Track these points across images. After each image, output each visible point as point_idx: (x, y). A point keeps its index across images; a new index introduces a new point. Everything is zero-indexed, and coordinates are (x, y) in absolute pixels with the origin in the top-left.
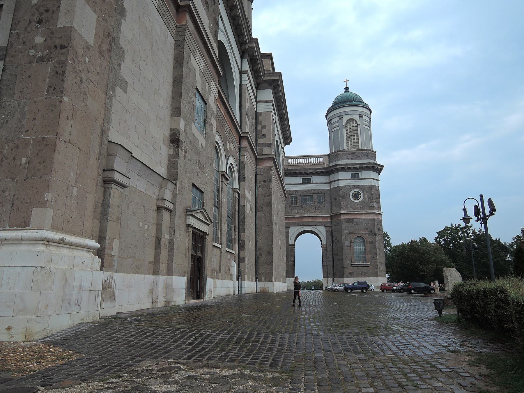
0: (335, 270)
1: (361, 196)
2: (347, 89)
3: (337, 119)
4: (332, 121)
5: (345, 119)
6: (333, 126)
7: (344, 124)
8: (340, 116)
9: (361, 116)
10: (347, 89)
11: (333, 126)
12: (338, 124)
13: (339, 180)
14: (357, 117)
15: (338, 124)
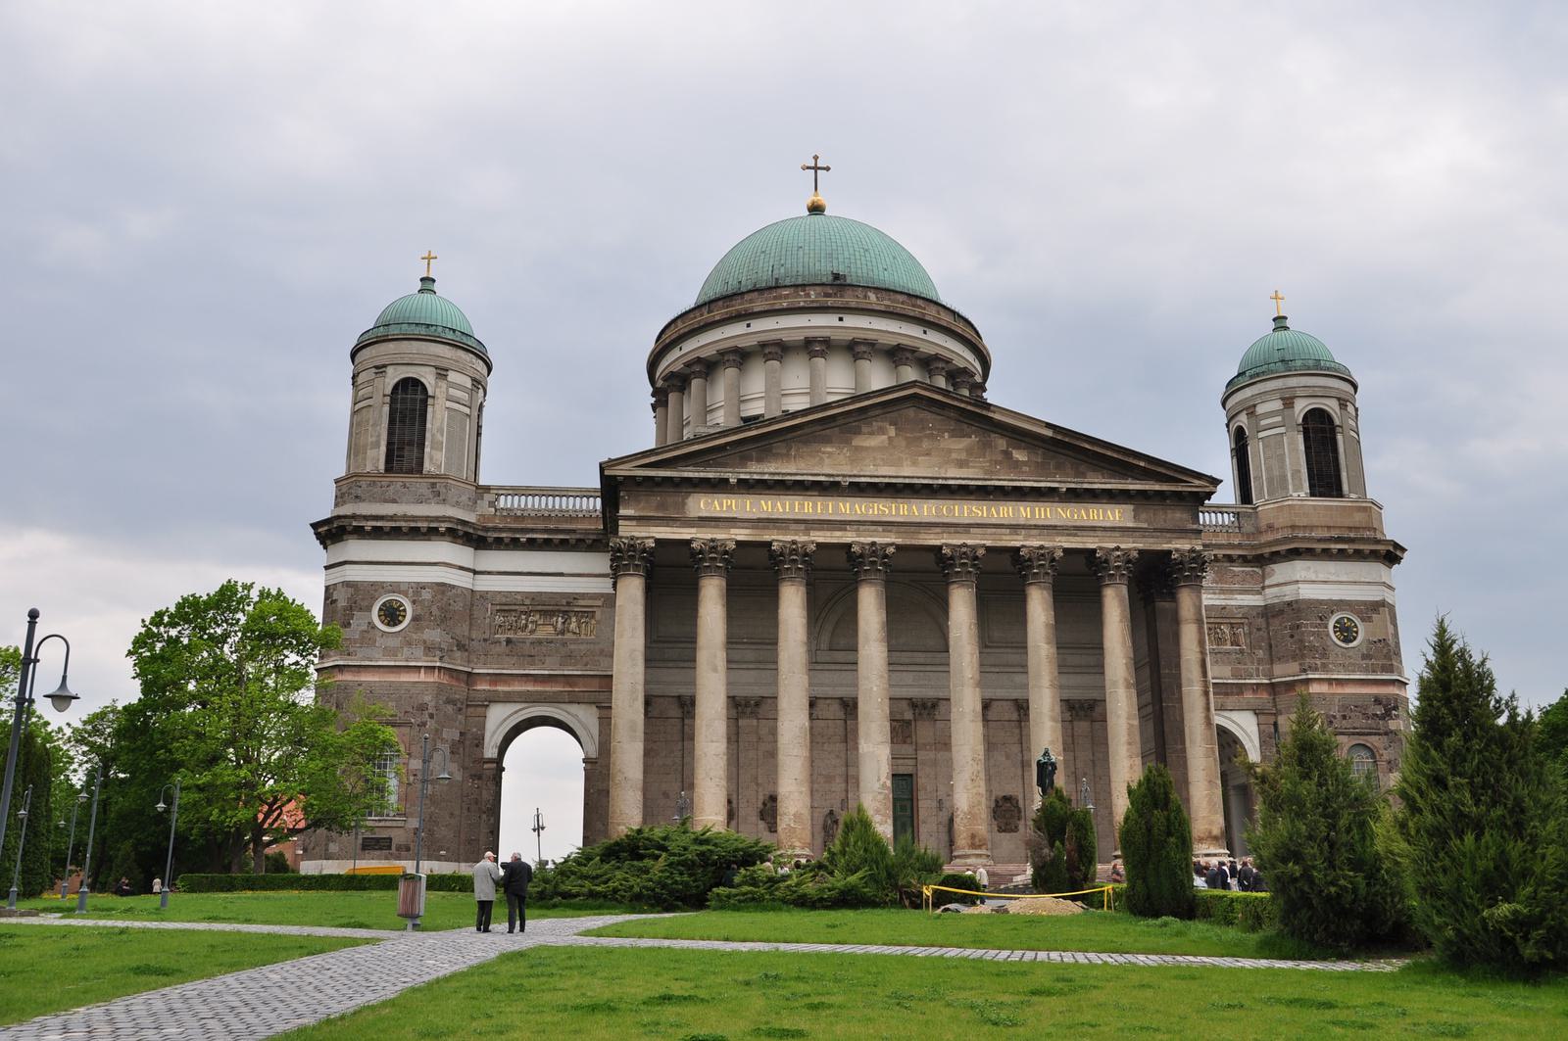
0: (924, 822)
1: (1357, 632)
2: (1280, 323)
3: (1277, 405)
4: (1260, 410)
5: (1301, 407)
6: (1263, 423)
7: (1300, 421)
8: (1287, 398)
9: (1343, 403)
10: (1280, 323)
11: (1263, 423)
12: (1279, 419)
13: (1297, 582)
14: (1331, 406)
15: (1279, 419)
